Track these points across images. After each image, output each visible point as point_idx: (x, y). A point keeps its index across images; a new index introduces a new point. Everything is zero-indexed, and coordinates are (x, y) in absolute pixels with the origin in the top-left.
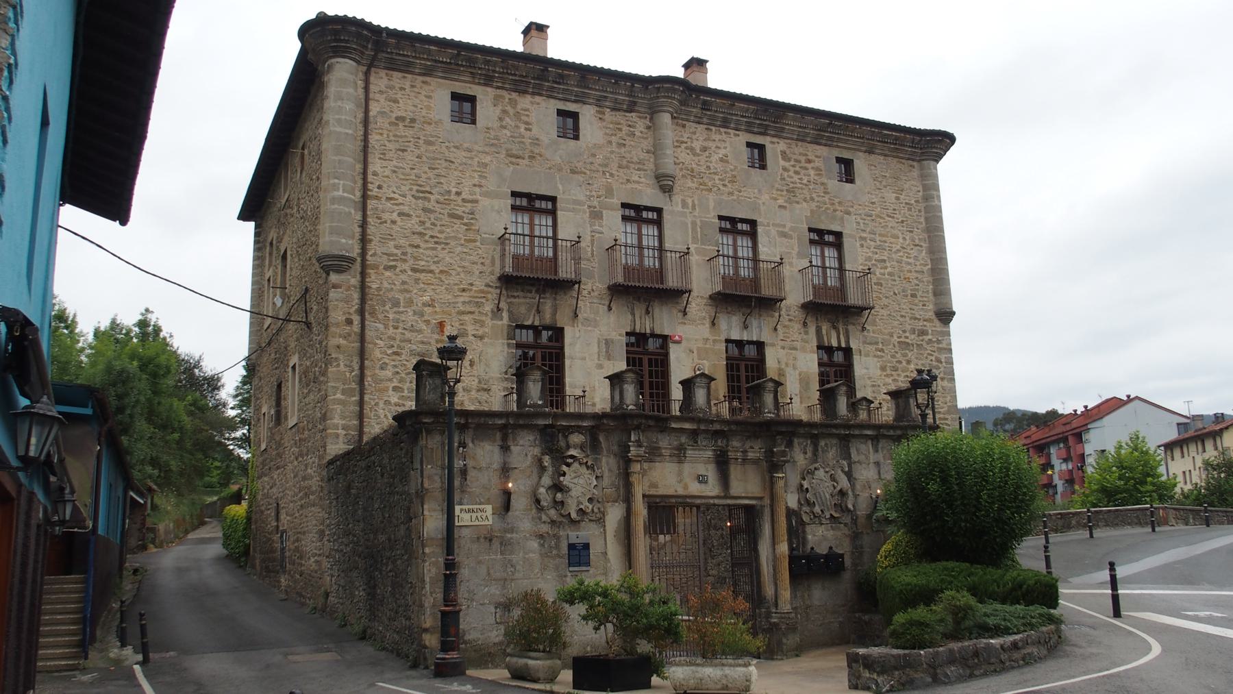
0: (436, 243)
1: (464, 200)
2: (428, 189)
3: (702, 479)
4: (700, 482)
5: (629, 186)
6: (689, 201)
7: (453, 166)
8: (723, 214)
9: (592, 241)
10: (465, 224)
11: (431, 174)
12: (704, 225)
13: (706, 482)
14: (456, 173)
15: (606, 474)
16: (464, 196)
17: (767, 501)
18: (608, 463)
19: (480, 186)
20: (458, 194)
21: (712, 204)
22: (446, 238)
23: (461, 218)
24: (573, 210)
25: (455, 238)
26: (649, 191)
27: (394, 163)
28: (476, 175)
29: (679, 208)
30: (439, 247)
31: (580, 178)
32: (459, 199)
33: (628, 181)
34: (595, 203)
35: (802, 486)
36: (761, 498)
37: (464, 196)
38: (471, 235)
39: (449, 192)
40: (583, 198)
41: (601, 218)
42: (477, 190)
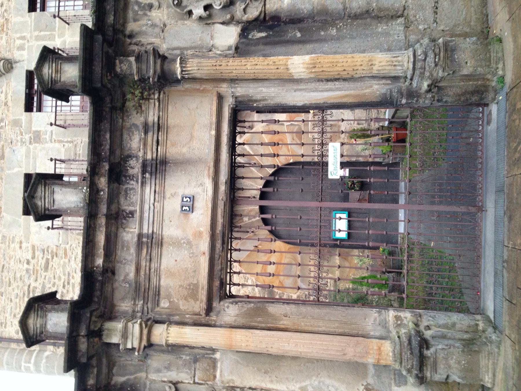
0: (68, 283)
1: (33, 258)
2: (26, 288)
3: (189, 206)
4: (192, 209)
5: (10, 104)
6: (18, 42)
7: (7, 265)
8: (26, 6)
9: (60, 142)
10: (53, 258)
11: (14, 285)
12: (38, 28)
13: (192, 199)
14: (12, 263)
15: (173, 375)
16: (29, 257)
17: (224, 88)
18: (158, 371)
19: (21, 242)
20: (28, 263)
21: (19, 19)
22: (64, 275)
23: (47, 260)
24: (35, 158)
25: (64, 266)
26: (13, 84)
27: (8, 315)
28: (12, 246)
29: (25, 53)
30: (72, 281)
31: (7, 151)
32: (33, 262)
33: (6, 104)
34: (27, 137)
35: (201, 18)
36: (220, 98)
37: (29, 257)
38: (61, 252)
39: (27, 271)
40: (23, 150)
41: (39, 132)
42: (24, 245)
